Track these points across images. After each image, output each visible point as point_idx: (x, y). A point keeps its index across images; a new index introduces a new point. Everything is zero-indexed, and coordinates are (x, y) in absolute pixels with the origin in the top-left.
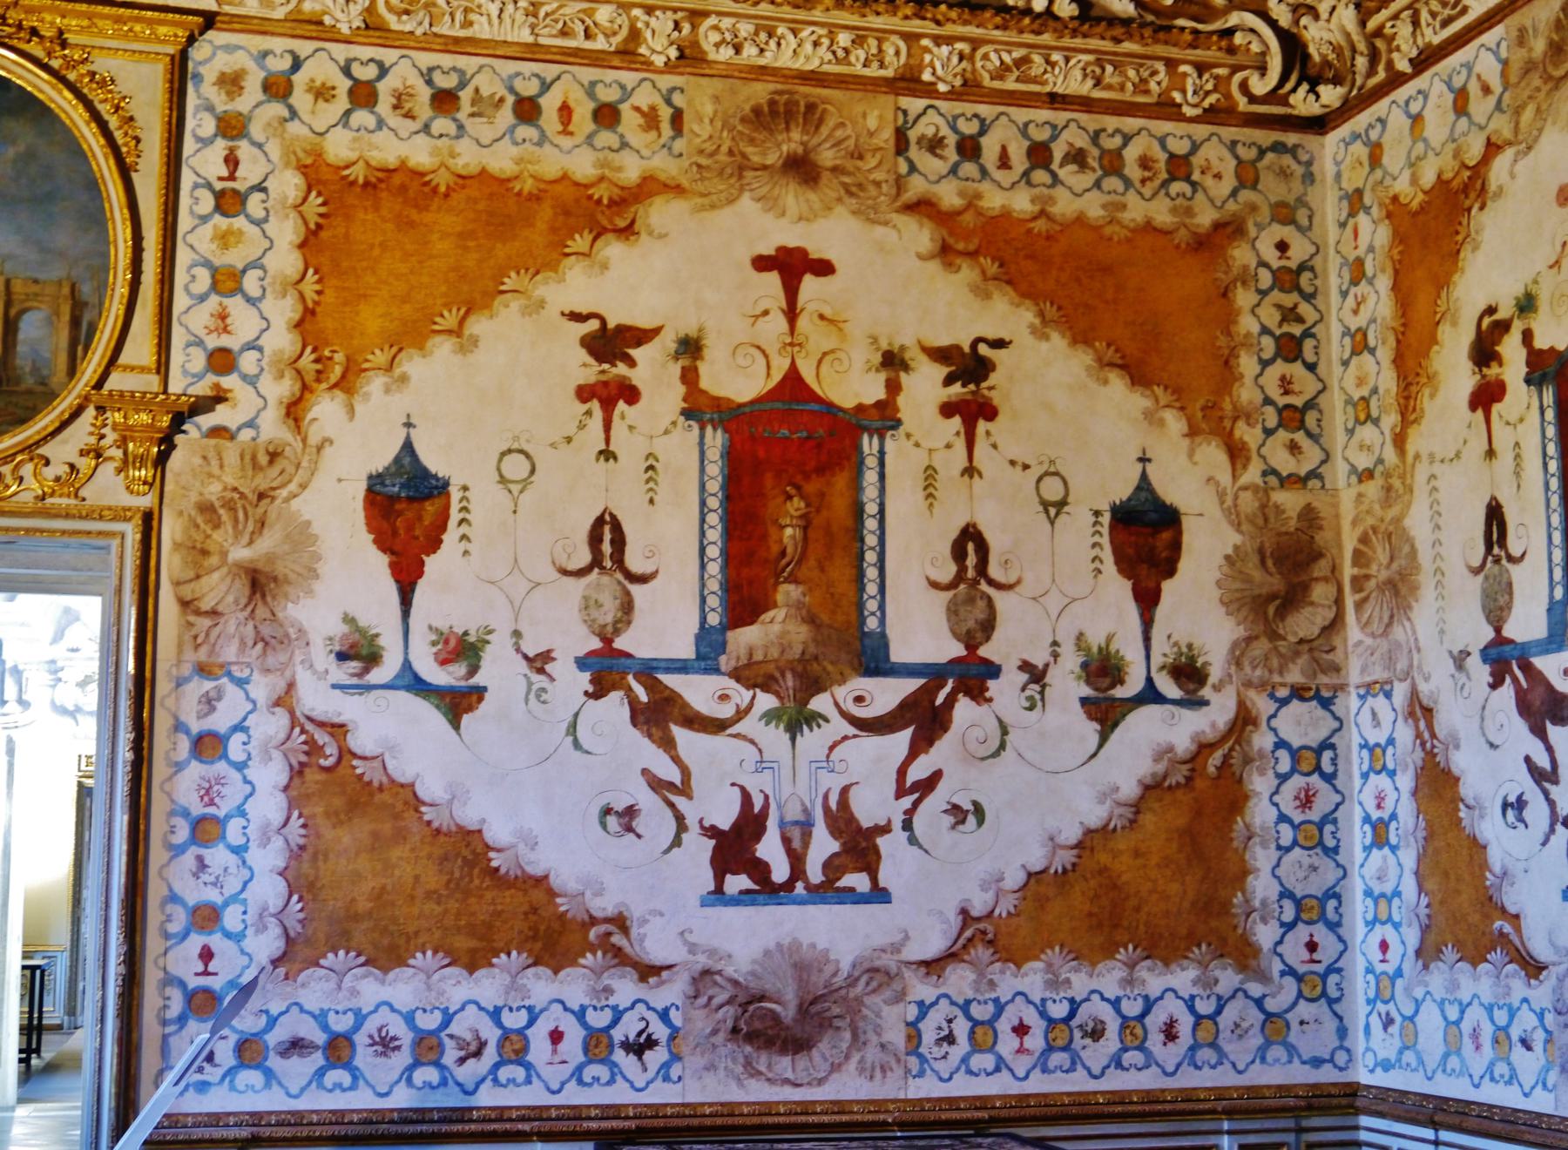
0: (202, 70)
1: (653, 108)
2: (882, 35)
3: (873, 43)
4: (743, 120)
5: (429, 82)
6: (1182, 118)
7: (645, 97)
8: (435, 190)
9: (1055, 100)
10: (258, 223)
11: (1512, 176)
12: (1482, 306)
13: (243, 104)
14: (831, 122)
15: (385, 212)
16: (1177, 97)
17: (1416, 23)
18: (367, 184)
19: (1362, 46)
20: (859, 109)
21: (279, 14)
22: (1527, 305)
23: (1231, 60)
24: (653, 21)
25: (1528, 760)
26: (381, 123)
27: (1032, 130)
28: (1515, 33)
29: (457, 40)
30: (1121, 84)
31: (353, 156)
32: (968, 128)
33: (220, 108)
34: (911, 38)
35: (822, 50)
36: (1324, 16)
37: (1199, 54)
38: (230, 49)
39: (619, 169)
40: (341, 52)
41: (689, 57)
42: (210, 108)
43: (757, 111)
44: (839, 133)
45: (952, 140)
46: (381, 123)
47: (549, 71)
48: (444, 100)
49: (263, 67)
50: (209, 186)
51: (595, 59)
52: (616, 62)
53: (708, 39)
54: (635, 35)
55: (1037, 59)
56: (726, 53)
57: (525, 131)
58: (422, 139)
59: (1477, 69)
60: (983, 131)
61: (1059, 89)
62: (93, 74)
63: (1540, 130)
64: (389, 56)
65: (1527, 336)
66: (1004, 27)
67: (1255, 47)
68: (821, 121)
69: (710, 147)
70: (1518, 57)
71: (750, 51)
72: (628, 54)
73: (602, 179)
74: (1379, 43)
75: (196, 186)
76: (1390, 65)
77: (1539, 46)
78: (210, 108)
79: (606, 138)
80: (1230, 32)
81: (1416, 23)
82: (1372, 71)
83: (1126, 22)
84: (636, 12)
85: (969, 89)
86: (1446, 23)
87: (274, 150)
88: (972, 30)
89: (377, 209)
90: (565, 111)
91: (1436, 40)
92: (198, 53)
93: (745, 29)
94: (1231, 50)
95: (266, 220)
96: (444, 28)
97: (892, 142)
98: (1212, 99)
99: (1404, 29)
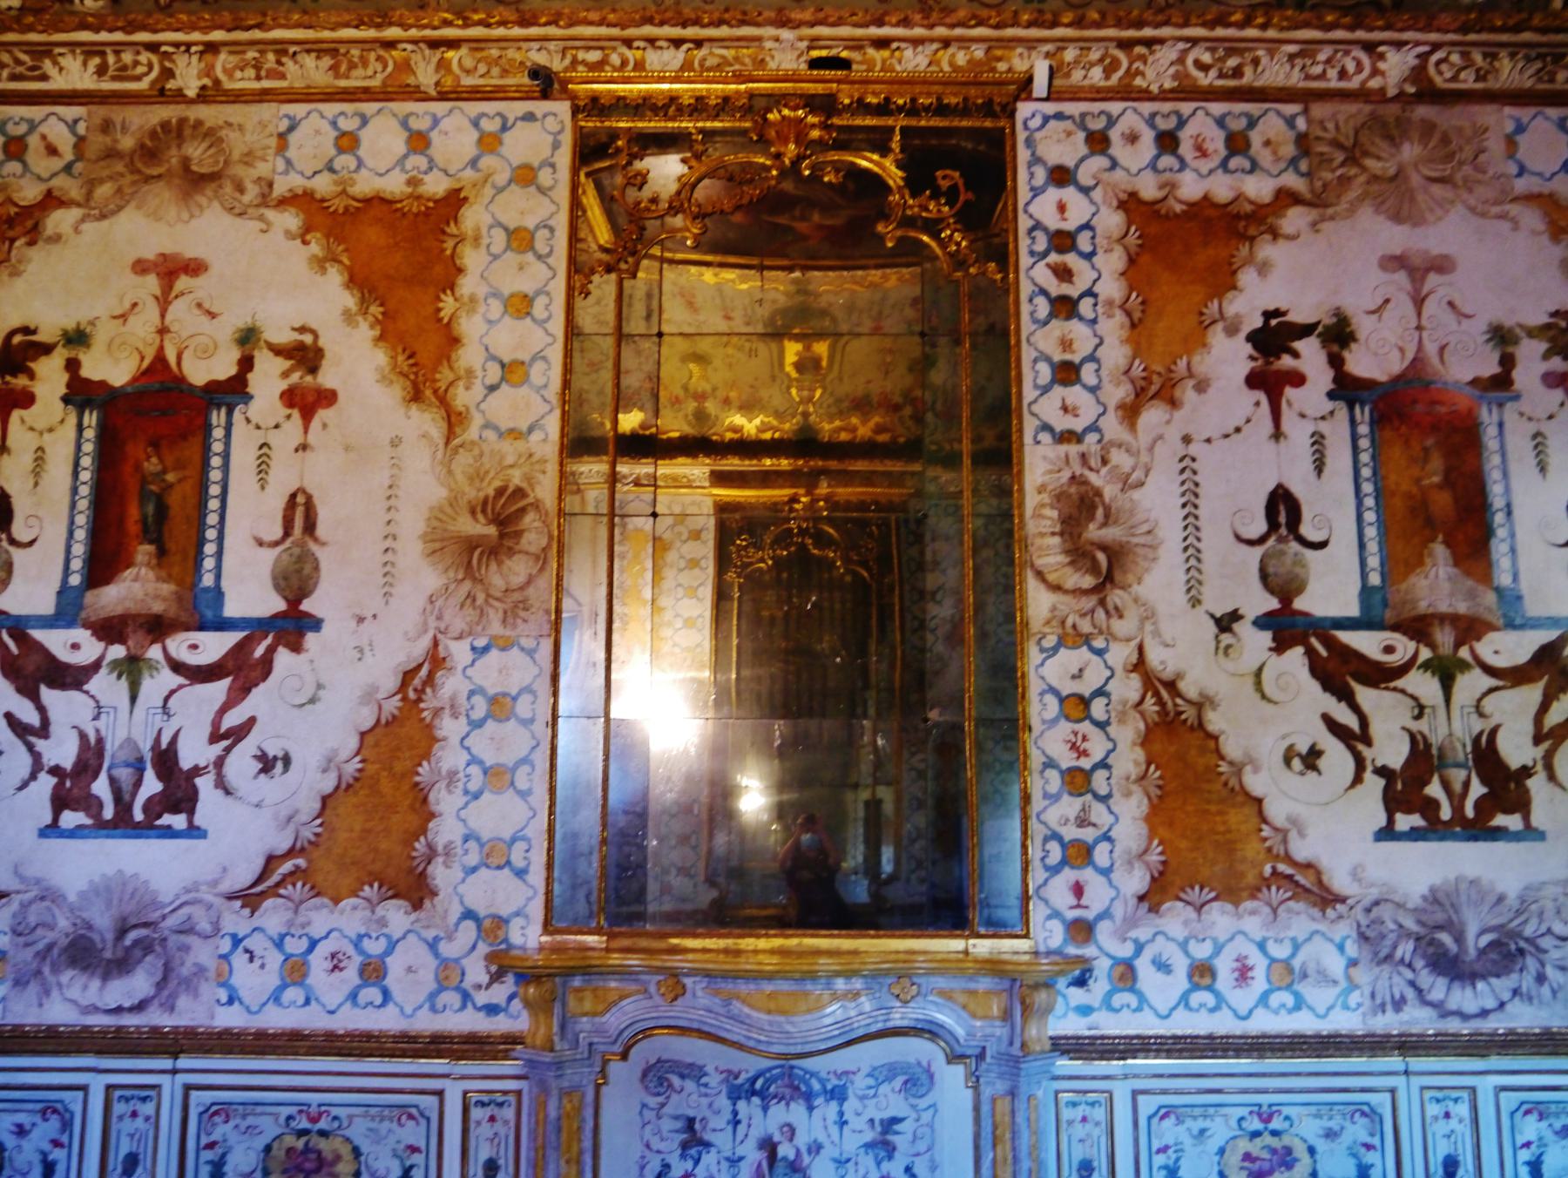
11: (77, 230)
12: (16, 322)
22: (78, 338)
25: (9, 717)
28: (97, 121)
63: (120, 208)
65: (72, 365)
70: (98, 142)
77: (127, 143)
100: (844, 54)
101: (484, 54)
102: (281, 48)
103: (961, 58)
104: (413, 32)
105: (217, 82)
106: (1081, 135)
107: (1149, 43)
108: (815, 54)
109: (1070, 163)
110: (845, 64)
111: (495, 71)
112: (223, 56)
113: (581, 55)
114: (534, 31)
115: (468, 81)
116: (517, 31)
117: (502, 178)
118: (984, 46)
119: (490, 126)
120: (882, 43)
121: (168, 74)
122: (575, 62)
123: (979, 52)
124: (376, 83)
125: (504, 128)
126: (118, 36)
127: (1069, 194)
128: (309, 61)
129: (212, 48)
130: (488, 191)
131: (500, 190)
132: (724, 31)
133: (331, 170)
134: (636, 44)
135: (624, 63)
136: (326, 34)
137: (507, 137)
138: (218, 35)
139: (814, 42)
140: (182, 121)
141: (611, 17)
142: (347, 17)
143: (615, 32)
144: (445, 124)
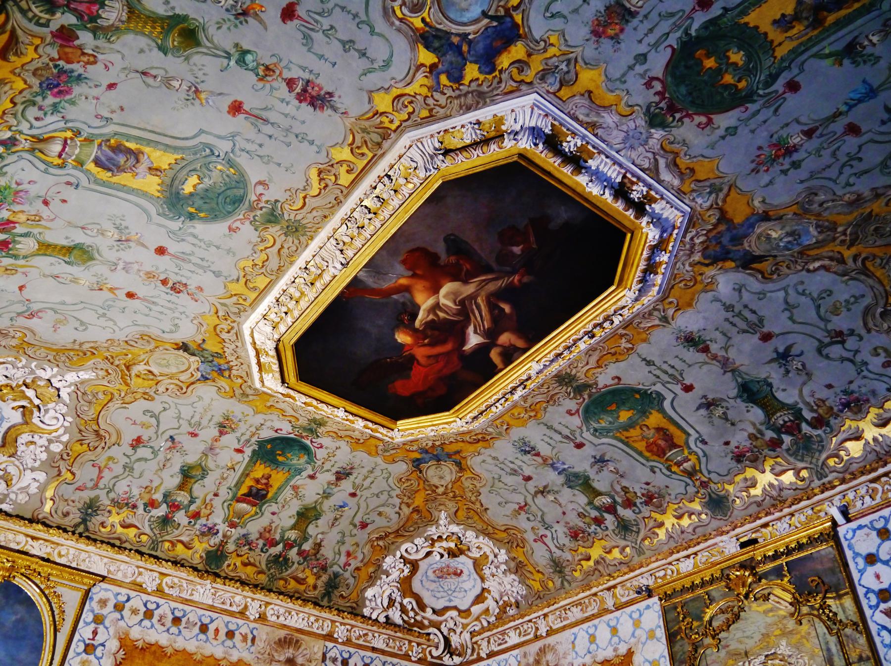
0: (94, 596)
1: (246, 634)
2: (324, 620)
3: (321, 621)
4: (275, 643)
5: (173, 613)
6: (411, 661)
7: (244, 630)
8: (166, 655)
9: (374, 649)
10: (98, 658)
13: (105, 612)
14: (303, 647)
15: (146, 661)
16: (410, 653)
17: (489, 642)
18: (142, 648)
19: (470, 646)
20: (312, 644)
21: (128, 580)
23: (429, 643)
24: (253, 604)
26: (152, 626)
27: (365, 658)
29: (187, 600)
30: (394, 646)
31: (140, 637)
32: (346, 656)
33: (96, 612)
34: (333, 622)
35: (305, 622)
36: (458, 633)
37: (419, 640)
38: (106, 590)
39: (231, 655)
40: (145, 597)
41: (262, 618)
42: (93, 611)
43: (280, 640)
44: (305, 652)
45: (340, 659)
46: (152, 626)
47: (215, 615)
48: (177, 621)
49: (116, 598)
50: (84, 641)
51: (231, 614)
52: (238, 616)
53: (269, 612)
54: (246, 607)
55: (370, 634)
56: (274, 618)
57: (202, 636)
58: (166, 634)
59: (509, 662)
60: (350, 657)
61: (375, 646)
62: (55, 592)
64: (161, 601)
66: (363, 623)
67: (436, 640)
68: (300, 647)
69: (262, 651)
70: (524, 662)
71: (282, 619)
72: (242, 614)
73: (225, 658)
74: (475, 646)
75: (79, 641)
76: (478, 654)
78: (93, 611)
79: (229, 643)
80: (429, 634)
81: (489, 642)
82: (472, 654)
83: (399, 626)
84: (249, 600)
85: (348, 642)
86: (500, 645)
87: (111, 630)
88: (353, 622)
89: (143, 659)
90: (217, 630)
91: (495, 649)
92: (94, 590)
93: (282, 611)
94: (429, 640)
95: (101, 658)
96: (183, 595)
97: (321, 659)
98: (421, 655)
99: (484, 644)
100: (754, 536)
102: (565, 608)
104: (601, 588)
105: (551, 627)
106: (874, 533)
109: (874, 551)
110: (754, 541)
112: (550, 617)
113: (657, 575)
114: (637, 572)
115: (624, 600)
116: (632, 574)
117: (643, 639)
119: (636, 616)
120: (765, 525)
121: (537, 629)
124: (596, 611)
125: (641, 615)
126: (521, 621)
127: (879, 567)
128: (574, 609)
129: (545, 615)
130: (640, 646)
131: (644, 644)
132: (702, 546)
133: (590, 652)
135: (673, 572)
136: (575, 598)
137: (642, 619)
138: (546, 610)
140: (545, 646)
141: (660, 557)
142: (578, 590)
143: (664, 562)
144: (621, 620)
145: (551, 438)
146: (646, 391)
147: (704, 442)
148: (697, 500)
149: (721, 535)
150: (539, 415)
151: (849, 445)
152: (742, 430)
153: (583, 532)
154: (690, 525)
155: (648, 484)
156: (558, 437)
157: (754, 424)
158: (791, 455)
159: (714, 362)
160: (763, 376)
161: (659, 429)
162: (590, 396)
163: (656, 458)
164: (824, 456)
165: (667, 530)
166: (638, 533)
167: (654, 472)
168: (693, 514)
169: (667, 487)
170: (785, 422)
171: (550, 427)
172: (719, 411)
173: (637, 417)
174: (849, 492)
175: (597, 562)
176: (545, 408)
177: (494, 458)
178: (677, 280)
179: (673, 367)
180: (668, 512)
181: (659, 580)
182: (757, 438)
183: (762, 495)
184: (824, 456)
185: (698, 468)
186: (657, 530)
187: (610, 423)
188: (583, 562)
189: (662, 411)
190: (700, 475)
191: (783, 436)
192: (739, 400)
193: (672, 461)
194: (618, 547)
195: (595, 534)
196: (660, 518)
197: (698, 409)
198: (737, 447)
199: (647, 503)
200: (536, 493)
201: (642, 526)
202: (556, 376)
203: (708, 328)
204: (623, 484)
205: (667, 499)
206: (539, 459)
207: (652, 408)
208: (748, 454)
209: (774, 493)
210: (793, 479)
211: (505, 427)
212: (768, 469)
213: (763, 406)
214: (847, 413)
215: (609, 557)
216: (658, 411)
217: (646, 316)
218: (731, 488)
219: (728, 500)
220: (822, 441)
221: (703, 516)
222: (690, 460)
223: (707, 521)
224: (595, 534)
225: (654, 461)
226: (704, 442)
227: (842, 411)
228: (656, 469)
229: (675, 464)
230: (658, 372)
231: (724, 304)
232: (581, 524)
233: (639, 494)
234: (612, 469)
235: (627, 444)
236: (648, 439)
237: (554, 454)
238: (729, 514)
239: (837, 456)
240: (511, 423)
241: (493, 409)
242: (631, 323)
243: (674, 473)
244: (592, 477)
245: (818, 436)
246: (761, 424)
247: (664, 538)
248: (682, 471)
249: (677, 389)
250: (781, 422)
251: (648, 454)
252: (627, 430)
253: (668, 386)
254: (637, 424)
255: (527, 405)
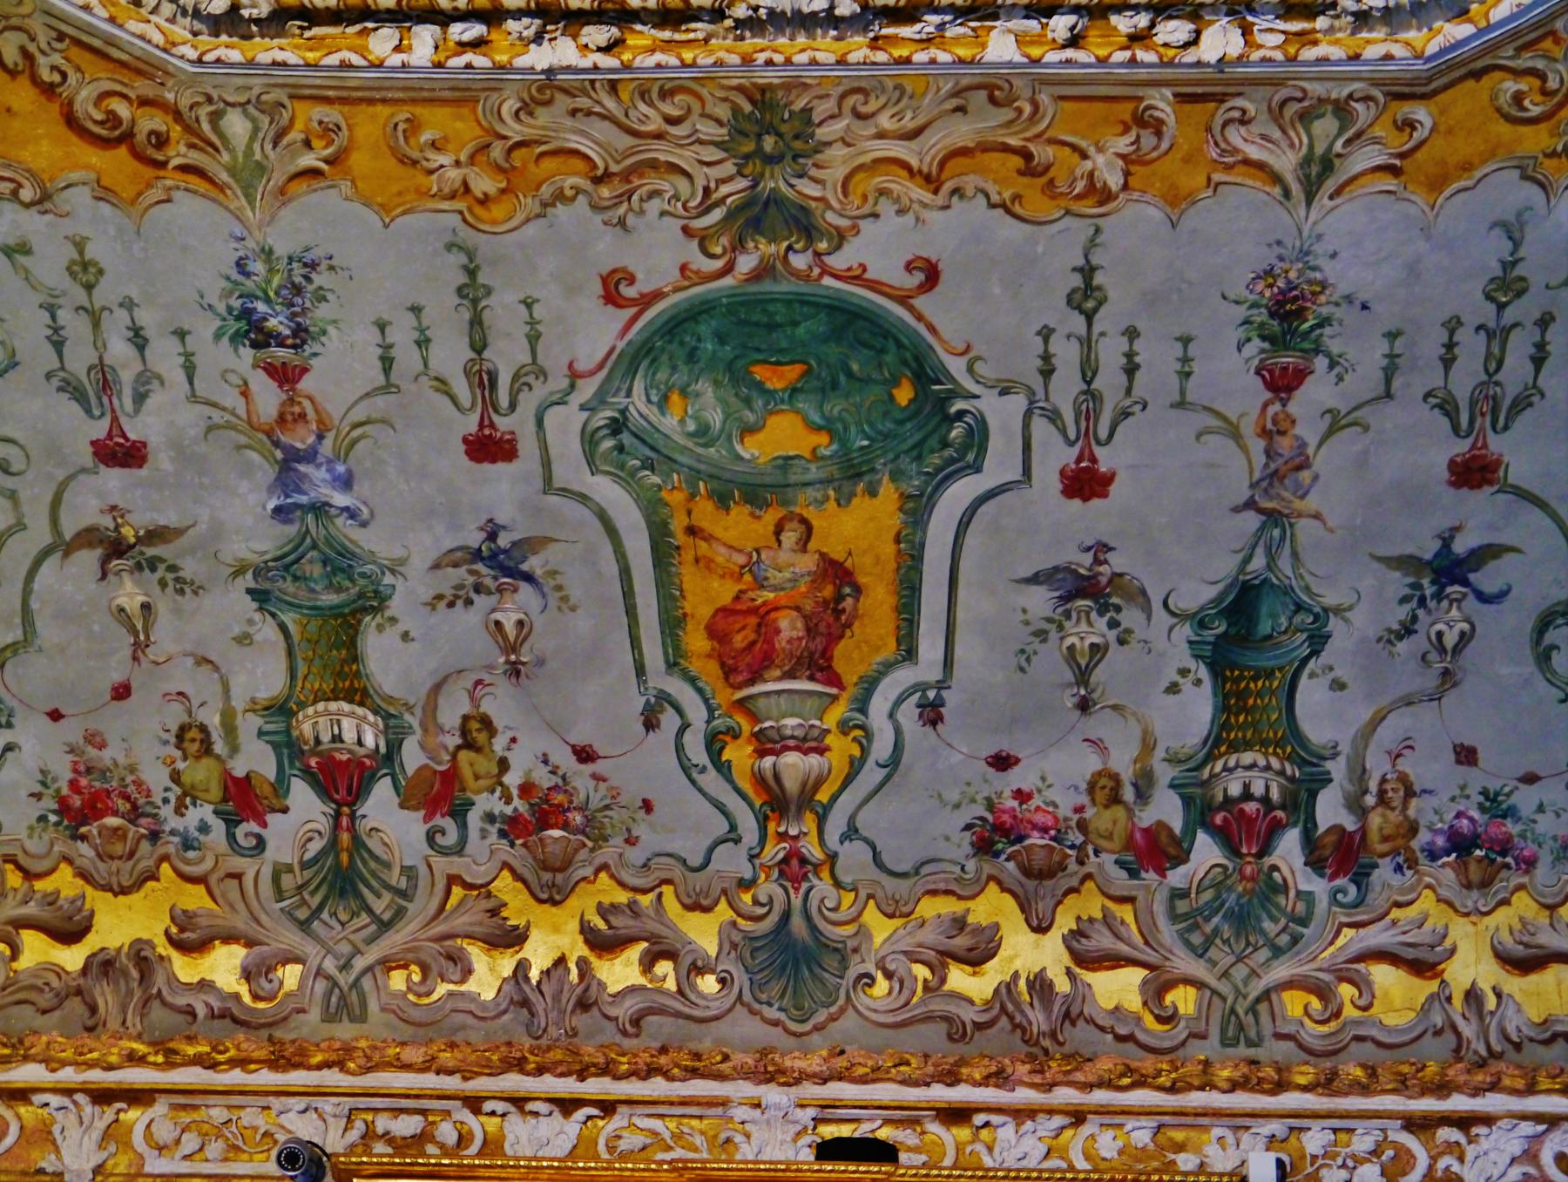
100: (884, 1133)
101: (196, 1116)
103: (1108, 1145)
104: (68, 1075)
107: (1464, 1122)
108: (829, 1131)
110: (885, 1152)
111: (215, 1148)
113: (382, 1123)
114: (298, 1078)
116: (266, 1078)
118: (1151, 1122)
120: (955, 1115)
122: (369, 1135)
123: (1141, 1134)
132: (657, 1087)
134: (488, 1106)
135: (463, 1140)
139: (827, 1111)
141: (446, 1057)
143: (452, 1083)
145: (423, 343)
146: (959, 393)
147: (932, 714)
148: (723, 912)
149: (768, 1077)
150: (497, 211)
151: (1382, 974)
152: (1096, 744)
153: (135, 814)
154: (632, 990)
155: (584, 755)
156: (451, 355)
157: (1148, 745)
158: (1174, 917)
159: (1257, 446)
160: (1330, 597)
161: (836, 573)
162: (763, 271)
163: (710, 671)
164: (1282, 971)
165: (522, 968)
166: (385, 926)
167: (650, 724)
168: (671, 955)
169: (647, 806)
170: (1247, 795)
171: (472, 292)
172: (1088, 630)
173: (814, 472)
174: (1316, 1125)
175: (103, 965)
176: (559, 197)
177: (85, 271)
178: (1525, 61)
179: (1131, 369)
180: (573, 903)
181: (380, 1148)
182: (1115, 799)
183: (988, 1006)
184: (1282, 971)
185: (823, 796)
186: (477, 954)
187: (702, 432)
188: (30, 939)
189: (917, 509)
190: (809, 823)
191: (1202, 838)
192: (1186, 631)
193: (754, 718)
194: (250, 943)
195: (187, 845)
196: (517, 905)
197: (1035, 579)
198: (1022, 796)
199: (512, 828)
200: (88, 537)
201: (422, 906)
202: (761, 96)
203: (1376, 307)
204: (487, 707)
205: (607, 853)
206: (268, 398)
207: (896, 476)
208: (1036, 839)
209: (1038, 1019)
210: (1134, 1002)
211: (308, 160)
212: (1065, 922)
213: (1231, 702)
214: (1445, 874)
215: (185, 969)
216: (905, 497)
217: (1293, 108)
218: (880, 928)
219: (844, 964)
220: (1304, 922)
221: (709, 984)
222: (822, 751)
223: (715, 1008)
224: (187, 845)
225: (692, 681)
226: (932, 714)
227: (1433, 855)
228: (669, 720)
229: (758, 736)
230: (1067, 354)
231: (1508, 266)
232: (156, 778)
233: (512, 779)
234: (509, 620)
235: (663, 553)
236: (760, 584)
237: (358, 414)
238: (821, 1016)
239: (1323, 992)
240: (359, 161)
241: (382, 42)
242: (1220, 99)
243: (724, 769)
244: (395, 606)
245: (1307, 897)
246: (1172, 760)
247: (488, 995)
248: (759, 779)
249: (1055, 455)
250: (1235, 789)
251: (697, 641)
252: (722, 500)
253: (1040, 426)
254: (785, 503)
255: (515, 131)
